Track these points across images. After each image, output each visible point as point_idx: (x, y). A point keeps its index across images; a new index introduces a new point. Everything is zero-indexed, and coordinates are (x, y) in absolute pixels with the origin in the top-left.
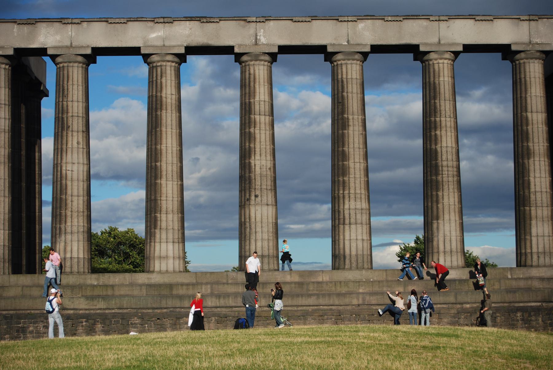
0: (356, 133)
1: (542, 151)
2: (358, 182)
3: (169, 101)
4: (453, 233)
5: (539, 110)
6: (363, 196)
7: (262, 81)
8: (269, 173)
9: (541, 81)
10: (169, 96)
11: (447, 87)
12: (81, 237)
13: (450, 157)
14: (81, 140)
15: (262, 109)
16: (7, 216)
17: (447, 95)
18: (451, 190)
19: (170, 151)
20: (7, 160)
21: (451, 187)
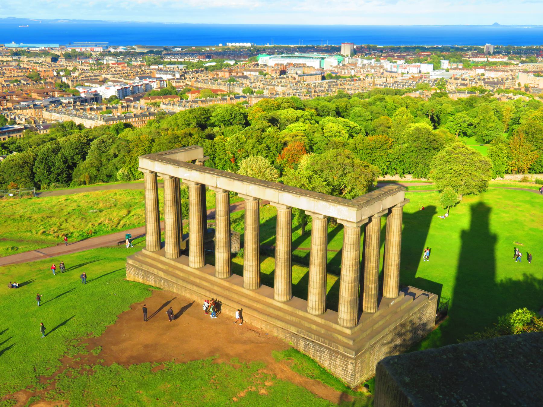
0: (249, 233)
1: (316, 264)
2: (249, 254)
3: (192, 202)
4: (280, 287)
5: (317, 244)
6: (251, 260)
7: (220, 202)
8: (222, 240)
9: (320, 230)
10: (192, 201)
11: (282, 223)
12: (171, 246)
13: (281, 254)
14: (170, 209)
15: (220, 214)
16: (154, 231)
17: (282, 226)
18: (280, 269)
19: (193, 222)
20: (153, 210)
21: (280, 267)
